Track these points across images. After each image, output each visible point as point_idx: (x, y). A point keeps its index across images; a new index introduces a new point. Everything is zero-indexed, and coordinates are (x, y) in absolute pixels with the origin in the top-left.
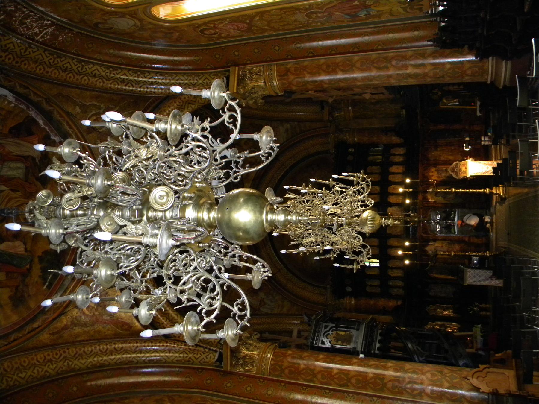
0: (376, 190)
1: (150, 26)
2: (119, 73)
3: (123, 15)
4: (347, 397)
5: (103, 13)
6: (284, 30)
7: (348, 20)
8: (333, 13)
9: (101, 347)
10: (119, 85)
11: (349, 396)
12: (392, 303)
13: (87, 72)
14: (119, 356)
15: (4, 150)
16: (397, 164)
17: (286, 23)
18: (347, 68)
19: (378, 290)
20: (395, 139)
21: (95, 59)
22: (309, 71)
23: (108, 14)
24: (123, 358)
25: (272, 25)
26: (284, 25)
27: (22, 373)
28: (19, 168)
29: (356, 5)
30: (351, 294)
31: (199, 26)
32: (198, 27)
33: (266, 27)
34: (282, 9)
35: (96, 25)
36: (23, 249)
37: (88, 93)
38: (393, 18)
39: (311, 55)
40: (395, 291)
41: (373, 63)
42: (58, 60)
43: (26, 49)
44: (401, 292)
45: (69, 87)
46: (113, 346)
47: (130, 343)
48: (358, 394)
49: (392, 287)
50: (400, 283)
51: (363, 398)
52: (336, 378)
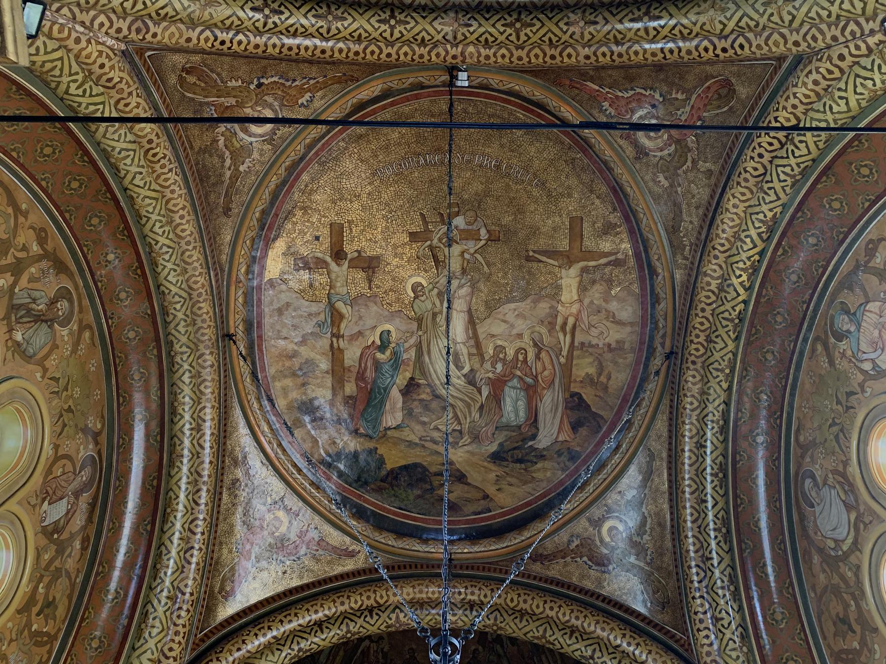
1: (849, 574)
2: (721, 547)
5: (841, 468)
9: (200, 523)
10: (696, 552)
14: (174, 553)
15: (544, 388)
21: (736, 496)
24: (168, 560)
27: (189, 378)
28: (517, 415)
36: (390, 424)
37: (666, 506)
43: (722, 371)
45: (669, 469)
46: (197, 546)
47: (195, 579)
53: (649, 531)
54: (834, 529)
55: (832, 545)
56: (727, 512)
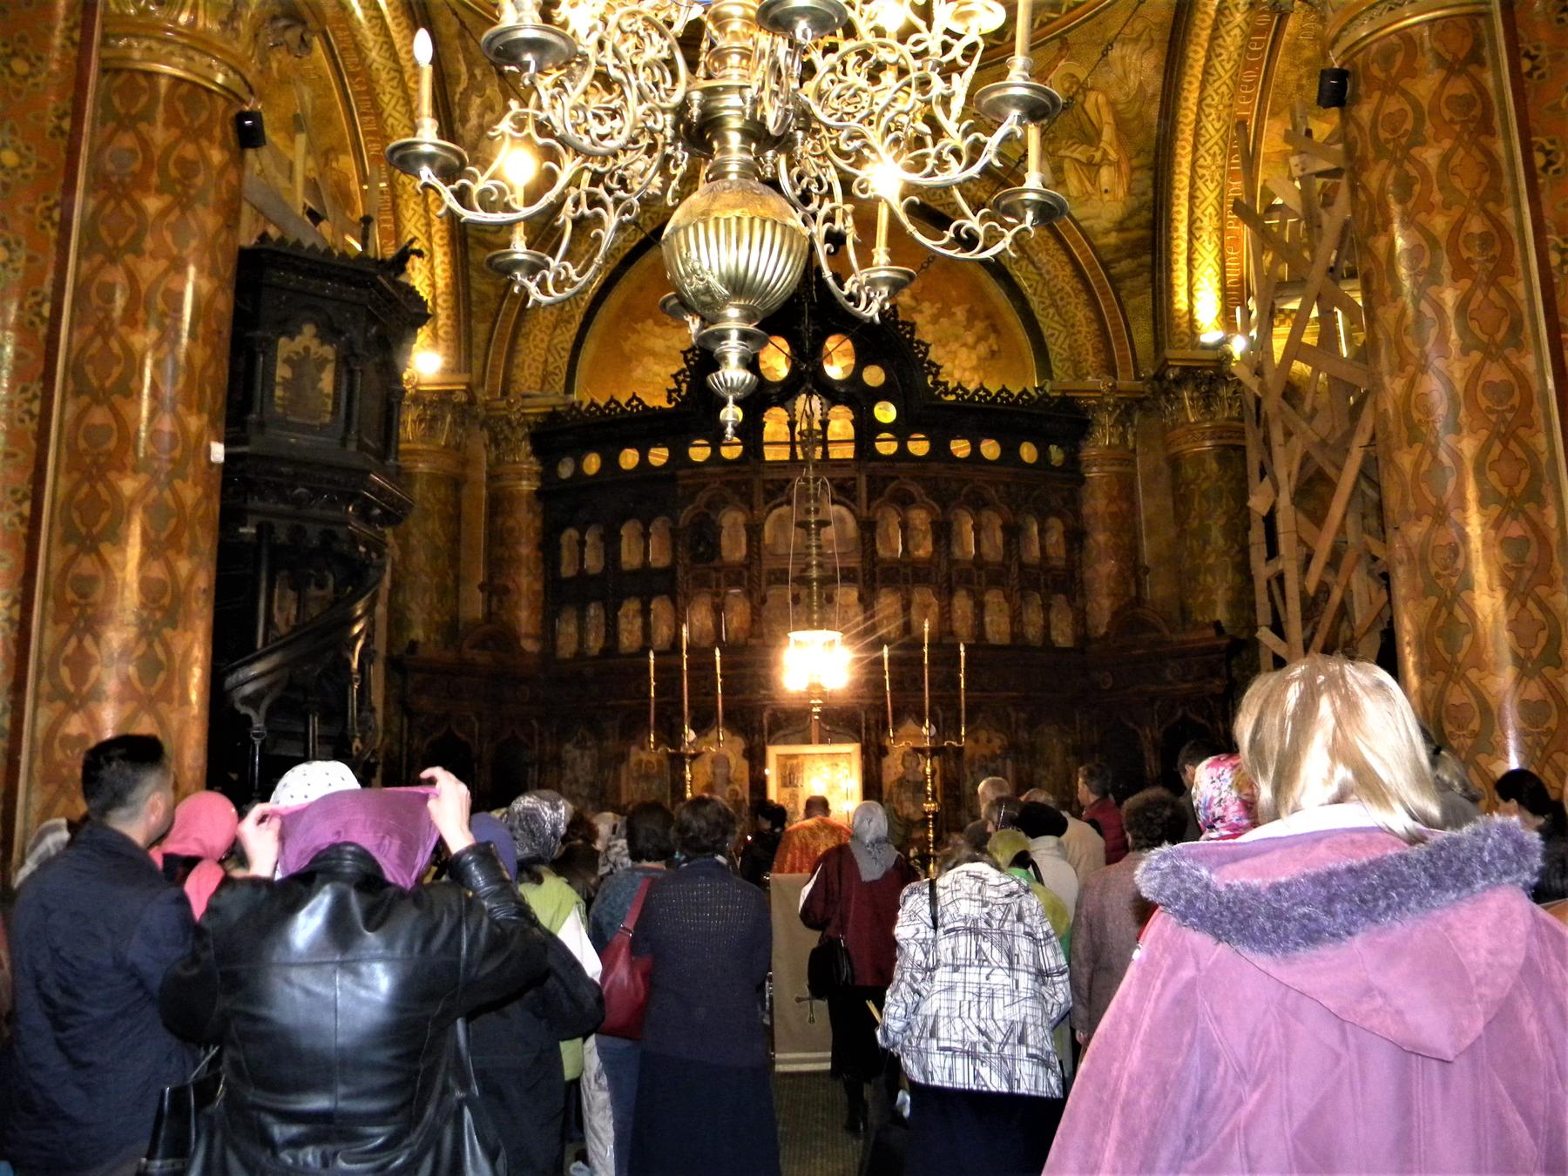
0: (917, 547)
4: (24, 390)
11: (29, 401)
12: (525, 618)
16: (1016, 618)
18: (1474, 325)
19: (567, 570)
20: (1102, 608)
22: (1455, 161)
30: (548, 475)
39: (1540, 160)
40: (567, 629)
41: (1505, 440)
44: (567, 645)
48: (42, 436)
49: (582, 618)
50: (595, 643)
51: (25, 457)
52: (106, 343)
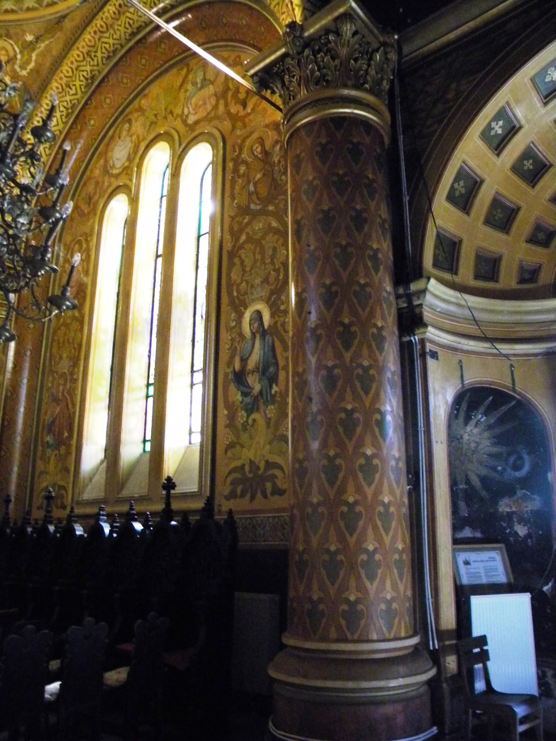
1: (106, 184)
3: (130, 159)
6: (53, 340)
7: (46, 421)
8: (59, 405)
13: (78, 80)
17: (61, 345)
23: (137, 142)
25: (63, 328)
26: (59, 343)
29: (63, 434)
31: (87, 241)
32: (87, 240)
33: (62, 320)
34: (80, 346)
35: (130, 121)
38: (37, 474)
42: (106, 55)
53: (28, 70)
54: (117, 159)
55: (111, 165)
56: (79, 103)
